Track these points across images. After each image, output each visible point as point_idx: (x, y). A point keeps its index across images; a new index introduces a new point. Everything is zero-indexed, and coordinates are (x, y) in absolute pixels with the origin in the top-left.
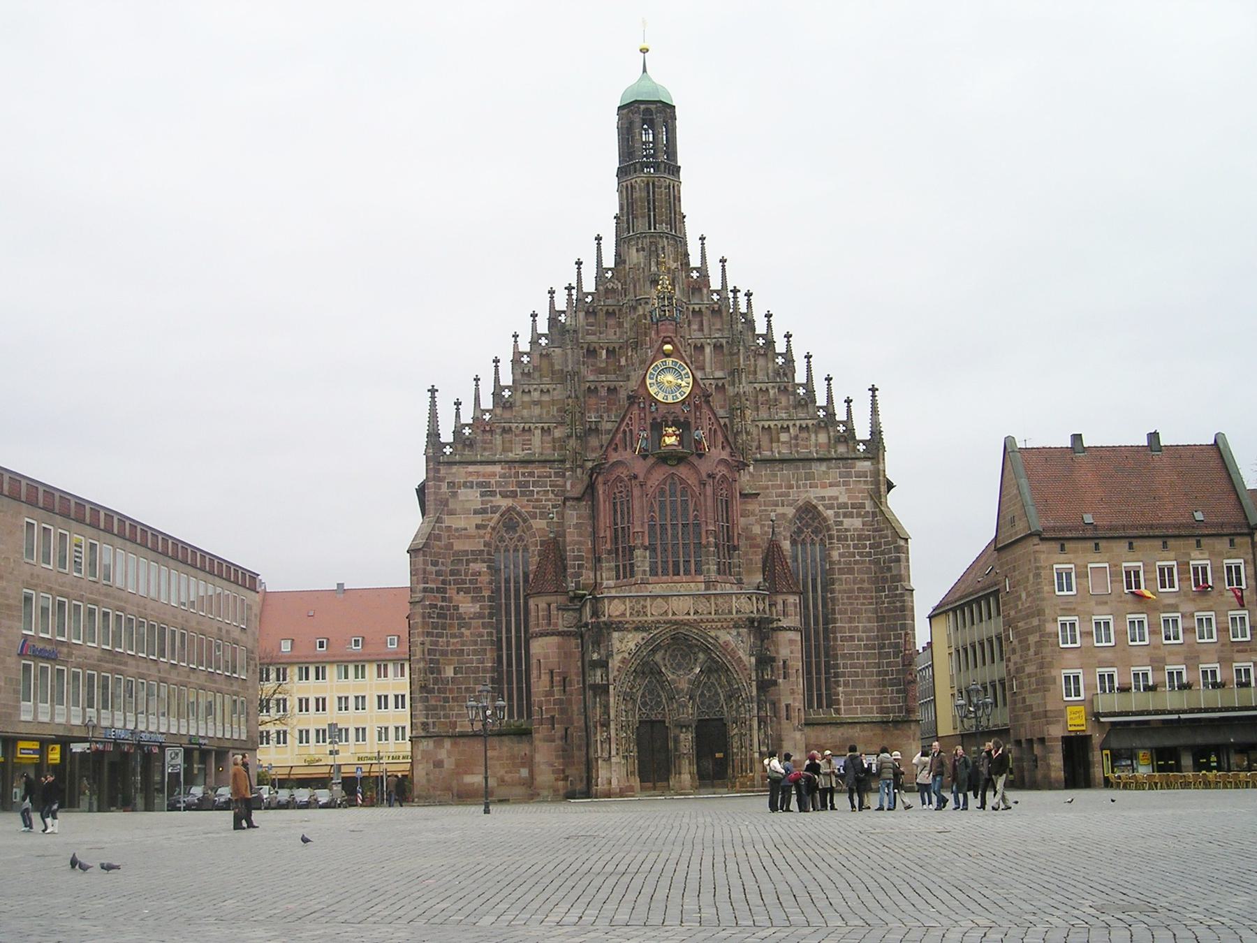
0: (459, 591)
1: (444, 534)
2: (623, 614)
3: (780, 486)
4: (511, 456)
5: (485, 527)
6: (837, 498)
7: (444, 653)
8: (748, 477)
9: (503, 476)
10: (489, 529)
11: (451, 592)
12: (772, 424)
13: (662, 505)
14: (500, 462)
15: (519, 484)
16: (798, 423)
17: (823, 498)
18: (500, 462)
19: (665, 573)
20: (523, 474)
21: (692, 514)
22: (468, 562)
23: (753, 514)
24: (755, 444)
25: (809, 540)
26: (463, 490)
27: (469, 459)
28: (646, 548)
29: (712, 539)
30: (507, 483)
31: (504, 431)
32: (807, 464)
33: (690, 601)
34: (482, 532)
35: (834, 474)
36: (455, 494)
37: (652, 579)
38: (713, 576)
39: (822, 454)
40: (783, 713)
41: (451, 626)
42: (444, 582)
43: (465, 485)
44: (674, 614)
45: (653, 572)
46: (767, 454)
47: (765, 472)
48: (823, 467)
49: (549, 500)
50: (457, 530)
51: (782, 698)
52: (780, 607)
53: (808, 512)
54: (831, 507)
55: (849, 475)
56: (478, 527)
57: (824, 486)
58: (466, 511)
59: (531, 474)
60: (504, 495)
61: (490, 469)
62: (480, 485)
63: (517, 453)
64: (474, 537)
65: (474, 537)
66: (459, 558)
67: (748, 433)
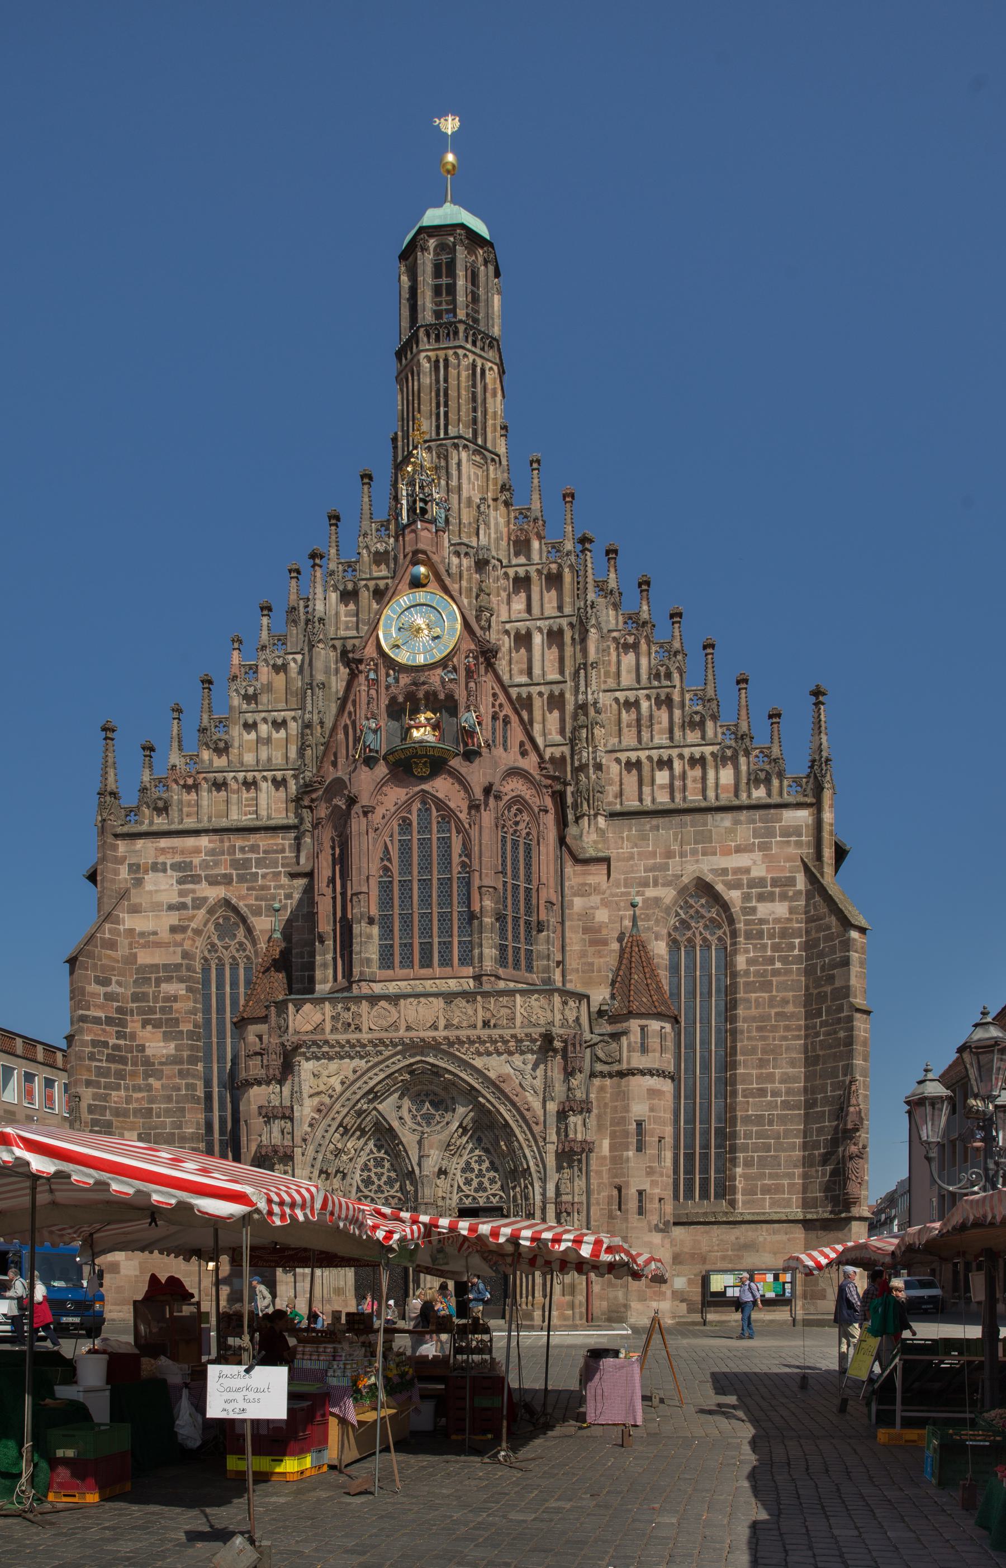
0: (145, 1023)
1: (123, 942)
2: (318, 1028)
3: (654, 854)
4: (224, 823)
5: (183, 929)
6: (747, 871)
7: (117, 1113)
8: (594, 837)
9: (212, 852)
10: (189, 932)
11: (134, 1025)
12: (643, 755)
13: (405, 848)
14: (206, 831)
15: (235, 864)
16: (687, 752)
17: (725, 871)
18: (206, 831)
19: (407, 962)
20: (242, 849)
21: (456, 859)
22: (158, 982)
23: (596, 889)
24: (612, 790)
25: (698, 941)
26: (151, 874)
27: (165, 828)
28: (371, 921)
29: (488, 903)
30: (217, 864)
31: (220, 786)
32: (698, 817)
33: (439, 1003)
34: (178, 937)
35: (743, 829)
36: (139, 882)
37: (380, 974)
38: (488, 965)
39: (726, 798)
40: (632, 1205)
41: (134, 1074)
42: (120, 1010)
43: (155, 867)
44: (409, 1028)
45: (386, 960)
46: (633, 804)
47: (631, 829)
48: (726, 820)
49: (281, 887)
50: (142, 934)
51: (632, 1180)
52: (635, 1036)
53: (704, 888)
54: (736, 885)
55: (770, 833)
56: (173, 929)
57: (727, 852)
58: (156, 907)
59: (254, 849)
60: (213, 881)
61: (190, 842)
62: (176, 867)
63: (237, 817)
64: (167, 945)
65: (167, 945)
66: (146, 975)
67: (599, 767)
